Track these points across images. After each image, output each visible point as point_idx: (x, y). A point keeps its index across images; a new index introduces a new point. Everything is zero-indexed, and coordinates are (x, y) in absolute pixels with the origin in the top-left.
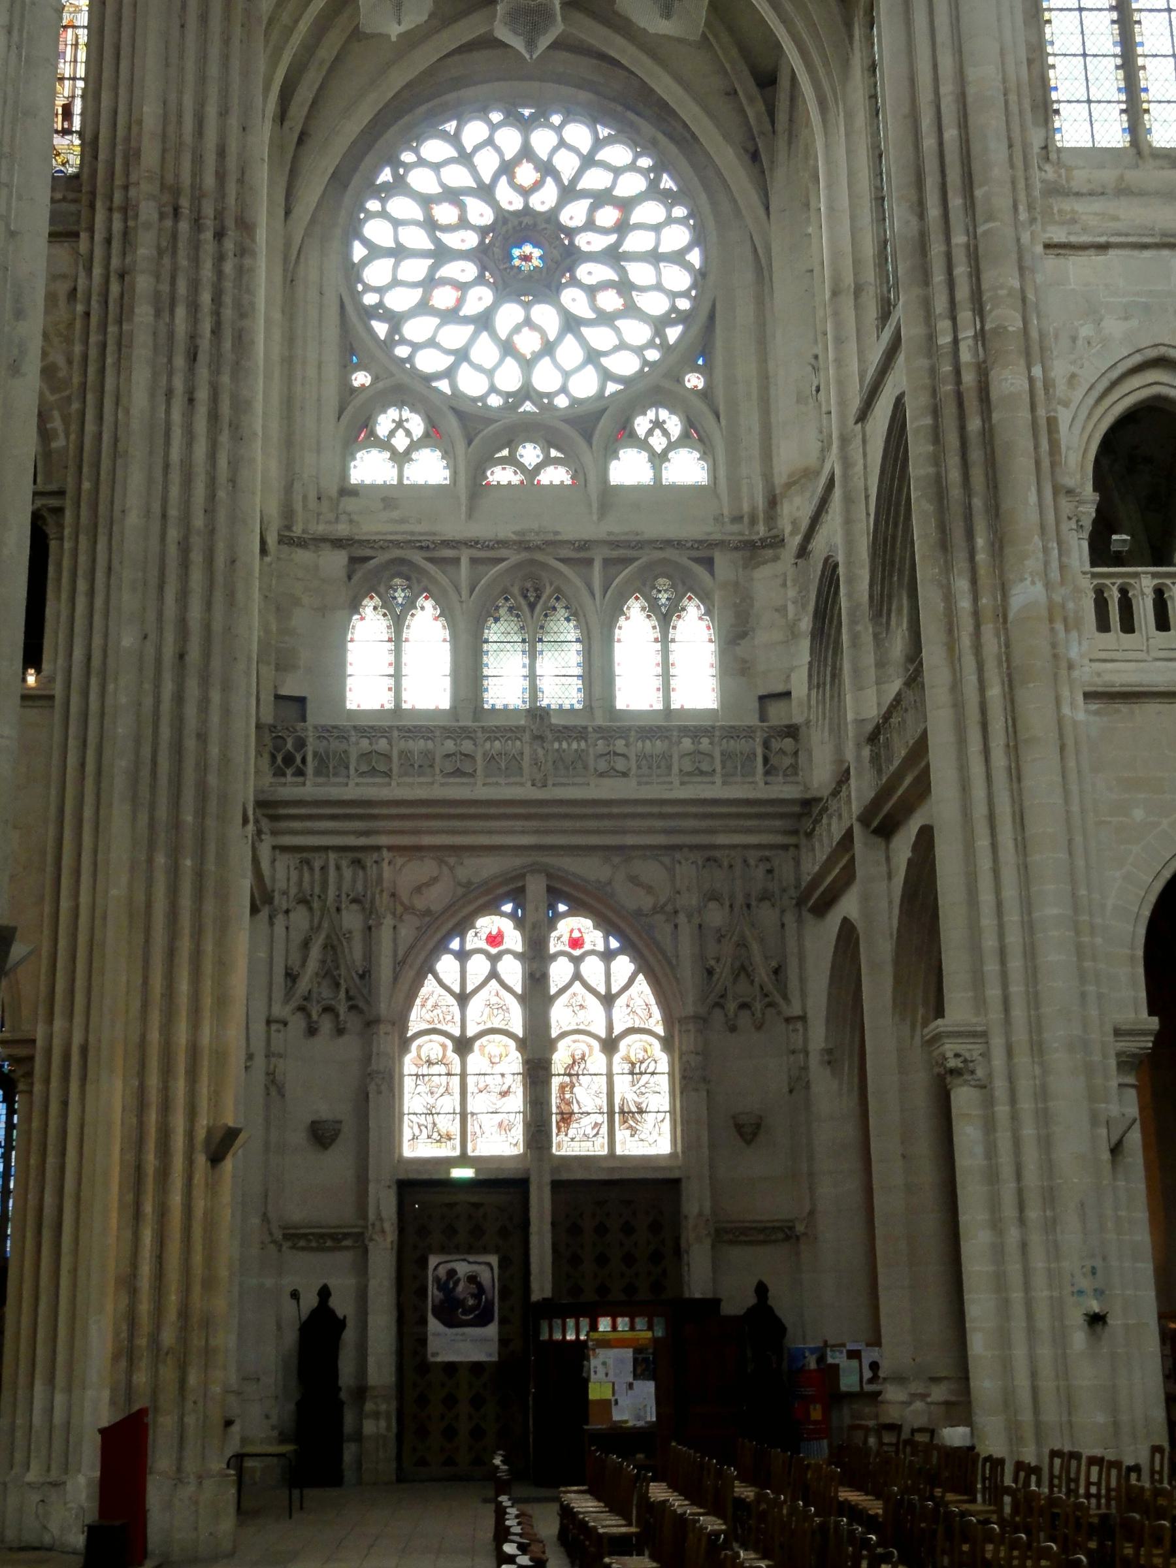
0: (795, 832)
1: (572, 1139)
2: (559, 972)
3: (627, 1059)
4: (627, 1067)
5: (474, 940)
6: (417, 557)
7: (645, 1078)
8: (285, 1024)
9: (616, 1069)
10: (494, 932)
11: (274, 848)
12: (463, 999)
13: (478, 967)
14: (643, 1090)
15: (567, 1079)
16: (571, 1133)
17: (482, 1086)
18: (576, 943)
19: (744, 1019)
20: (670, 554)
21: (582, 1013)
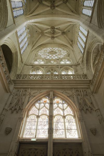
0: (89, 86)
1: (58, 135)
2: (55, 106)
3: (67, 119)
4: (67, 121)
5: (41, 101)
6: (40, 67)
7: (71, 123)
8: (7, 110)
9: (65, 121)
10: (45, 101)
11: (14, 88)
12: (39, 109)
13: (42, 105)
14: (71, 125)
15: (56, 123)
16: (57, 133)
17: (41, 124)
18: (58, 102)
19: (88, 112)
20: (67, 66)
21: (59, 112)
